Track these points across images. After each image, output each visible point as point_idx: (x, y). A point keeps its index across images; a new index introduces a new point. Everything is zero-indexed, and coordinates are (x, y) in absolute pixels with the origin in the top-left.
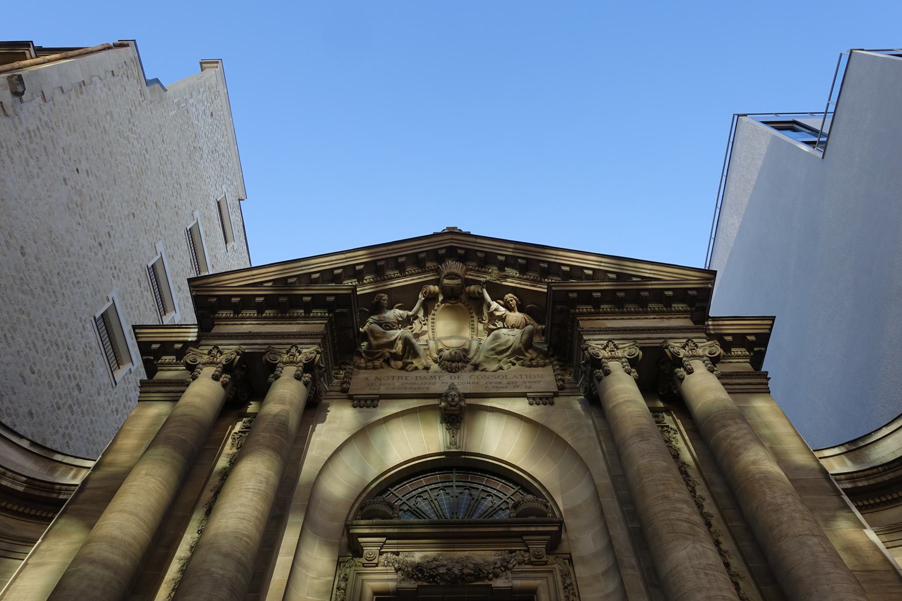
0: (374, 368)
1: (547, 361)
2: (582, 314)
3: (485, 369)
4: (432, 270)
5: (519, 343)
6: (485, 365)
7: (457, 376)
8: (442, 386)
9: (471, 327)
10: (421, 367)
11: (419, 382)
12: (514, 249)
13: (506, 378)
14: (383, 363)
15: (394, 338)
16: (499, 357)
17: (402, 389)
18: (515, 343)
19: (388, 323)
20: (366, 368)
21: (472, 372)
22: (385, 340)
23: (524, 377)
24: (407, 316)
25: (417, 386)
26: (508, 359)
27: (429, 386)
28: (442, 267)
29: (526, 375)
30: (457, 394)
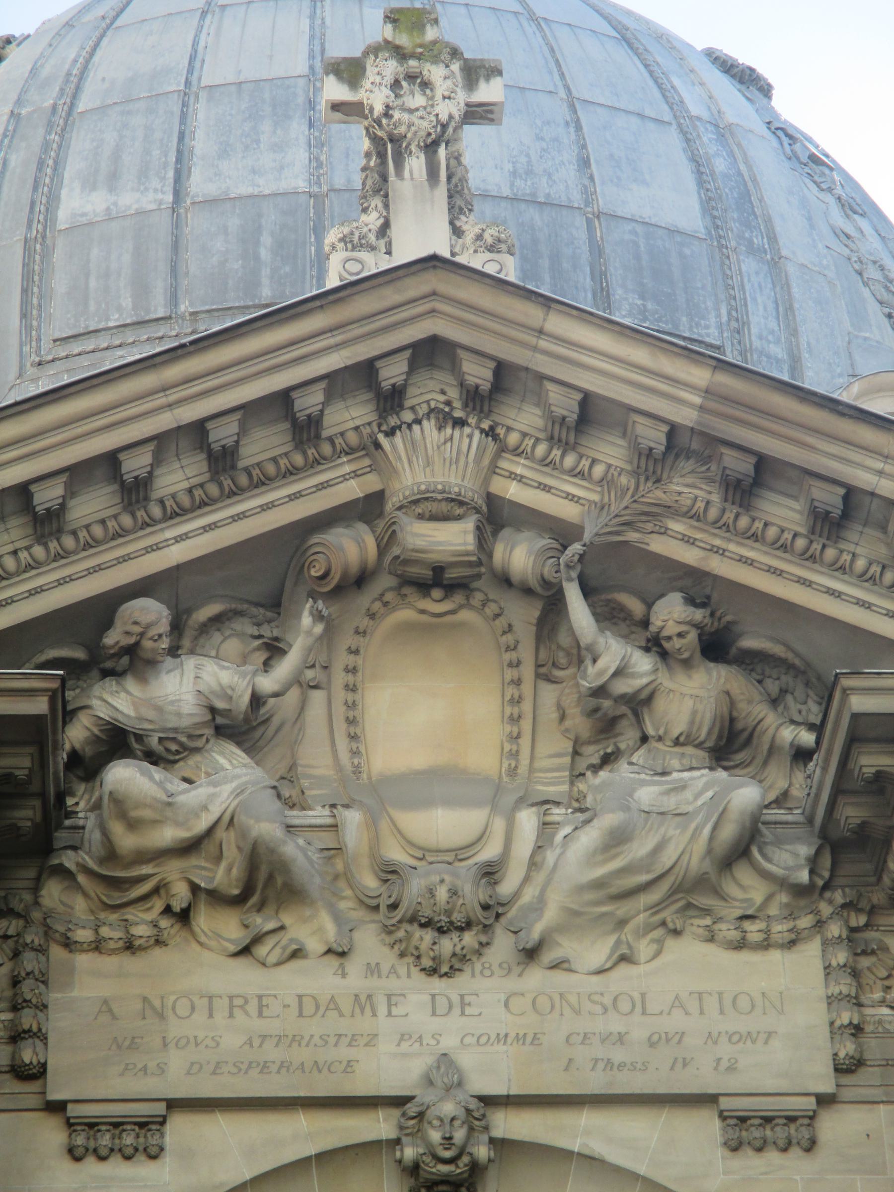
0: (130, 947)
1: (805, 922)
3: (565, 961)
4: (350, 451)
5: (703, 859)
7: (456, 999)
8: (404, 1055)
10: (314, 945)
11: (313, 1028)
13: (644, 1013)
14: (164, 923)
15: (202, 824)
16: (622, 909)
17: (254, 1073)
18: (686, 858)
19: (175, 730)
20: (97, 946)
21: (517, 970)
23: (712, 1004)
24: (257, 700)
28: (394, 447)
29: (720, 994)
30: (461, 1113)
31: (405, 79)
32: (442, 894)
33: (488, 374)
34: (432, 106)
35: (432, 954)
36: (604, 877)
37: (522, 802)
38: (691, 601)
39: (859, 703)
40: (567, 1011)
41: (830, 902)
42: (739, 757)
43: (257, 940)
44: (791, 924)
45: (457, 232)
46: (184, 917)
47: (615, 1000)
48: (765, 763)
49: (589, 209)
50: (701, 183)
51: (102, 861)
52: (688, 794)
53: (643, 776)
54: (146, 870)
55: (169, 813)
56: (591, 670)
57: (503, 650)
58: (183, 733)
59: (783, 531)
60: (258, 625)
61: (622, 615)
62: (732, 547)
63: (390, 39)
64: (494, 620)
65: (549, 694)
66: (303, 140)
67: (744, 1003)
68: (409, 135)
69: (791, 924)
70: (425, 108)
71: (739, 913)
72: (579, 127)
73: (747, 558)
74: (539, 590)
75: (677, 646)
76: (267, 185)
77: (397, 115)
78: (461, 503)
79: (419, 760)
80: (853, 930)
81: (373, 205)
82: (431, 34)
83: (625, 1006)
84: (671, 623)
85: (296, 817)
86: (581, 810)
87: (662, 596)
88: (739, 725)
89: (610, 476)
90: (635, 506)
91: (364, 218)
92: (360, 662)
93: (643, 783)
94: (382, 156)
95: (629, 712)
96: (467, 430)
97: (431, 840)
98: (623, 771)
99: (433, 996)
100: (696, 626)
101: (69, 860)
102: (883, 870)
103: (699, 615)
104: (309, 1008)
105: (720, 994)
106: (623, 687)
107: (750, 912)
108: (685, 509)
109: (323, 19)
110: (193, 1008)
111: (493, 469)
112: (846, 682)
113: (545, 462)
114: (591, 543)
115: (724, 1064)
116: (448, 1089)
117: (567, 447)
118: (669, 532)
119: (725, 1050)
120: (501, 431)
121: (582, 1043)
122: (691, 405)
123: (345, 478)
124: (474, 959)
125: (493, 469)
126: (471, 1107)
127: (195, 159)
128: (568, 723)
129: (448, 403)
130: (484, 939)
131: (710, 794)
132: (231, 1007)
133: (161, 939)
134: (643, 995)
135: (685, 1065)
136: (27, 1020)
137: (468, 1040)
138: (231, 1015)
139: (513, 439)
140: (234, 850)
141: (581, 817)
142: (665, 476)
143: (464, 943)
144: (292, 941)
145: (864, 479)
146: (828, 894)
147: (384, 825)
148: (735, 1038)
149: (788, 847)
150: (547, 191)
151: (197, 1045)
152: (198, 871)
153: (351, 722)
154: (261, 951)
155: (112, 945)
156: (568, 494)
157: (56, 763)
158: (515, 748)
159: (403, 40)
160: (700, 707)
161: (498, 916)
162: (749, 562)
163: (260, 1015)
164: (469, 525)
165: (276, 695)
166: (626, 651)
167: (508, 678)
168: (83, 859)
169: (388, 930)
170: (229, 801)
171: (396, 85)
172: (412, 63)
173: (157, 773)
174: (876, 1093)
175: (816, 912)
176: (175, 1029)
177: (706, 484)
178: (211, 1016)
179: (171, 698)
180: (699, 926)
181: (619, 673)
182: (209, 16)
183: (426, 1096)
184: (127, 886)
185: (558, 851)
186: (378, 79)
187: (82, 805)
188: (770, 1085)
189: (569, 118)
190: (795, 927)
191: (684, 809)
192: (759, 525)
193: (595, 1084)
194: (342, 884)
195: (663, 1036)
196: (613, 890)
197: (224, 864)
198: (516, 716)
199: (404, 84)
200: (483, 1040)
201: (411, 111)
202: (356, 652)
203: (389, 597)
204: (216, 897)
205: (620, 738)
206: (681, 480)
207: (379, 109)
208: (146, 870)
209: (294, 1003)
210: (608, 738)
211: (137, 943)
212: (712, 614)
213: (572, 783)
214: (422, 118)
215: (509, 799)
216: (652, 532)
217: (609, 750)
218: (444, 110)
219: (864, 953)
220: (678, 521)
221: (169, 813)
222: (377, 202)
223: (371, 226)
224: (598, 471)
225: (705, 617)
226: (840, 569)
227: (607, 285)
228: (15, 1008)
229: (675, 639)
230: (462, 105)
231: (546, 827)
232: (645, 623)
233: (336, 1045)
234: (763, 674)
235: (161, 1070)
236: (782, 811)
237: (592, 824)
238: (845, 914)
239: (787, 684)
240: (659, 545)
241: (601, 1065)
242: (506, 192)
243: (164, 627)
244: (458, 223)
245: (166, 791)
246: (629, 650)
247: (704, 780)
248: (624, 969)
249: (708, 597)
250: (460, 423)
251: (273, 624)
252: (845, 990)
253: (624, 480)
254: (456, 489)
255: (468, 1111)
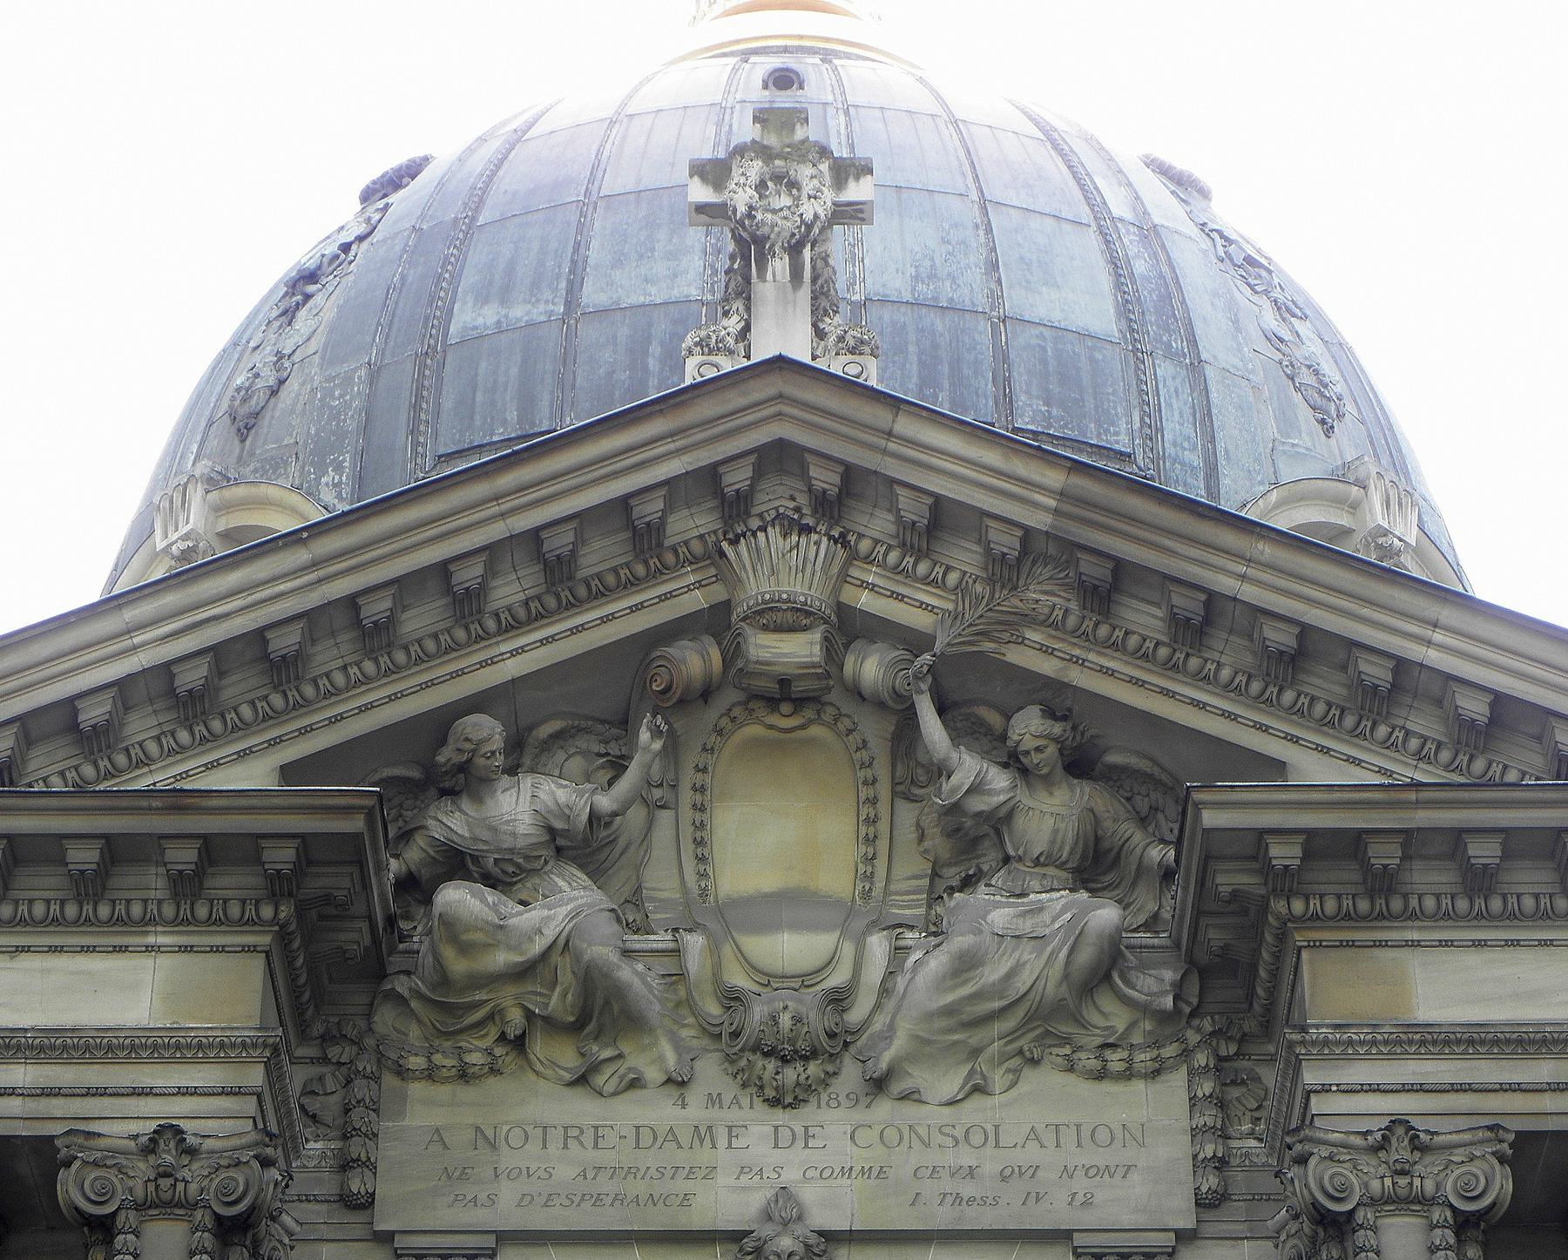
0: (464, 1075)
1: (1170, 1051)
2: (1315, 919)
4: (694, 560)
6: (915, 1071)
7: (799, 1130)
9: (863, 830)
12: (1063, 495)
13: (997, 1145)
14: (498, 1051)
15: (538, 946)
16: (975, 1038)
17: (587, 1205)
19: (511, 851)
21: (865, 1100)
22: (501, 959)
23: (1069, 1137)
24: (594, 818)
25: (638, 1187)
26: (1010, 1042)
27: (688, 1186)
28: (738, 554)
29: (1078, 1126)
30: (800, 1249)
31: (771, 179)
32: (785, 1021)
33: (836, 479)
34: (797, 206)
35: (775, 1084)
36: (952, 1003)
37: (874, 926)
38: (1050, 714)
39: (1210, 818)
40: (916, 1143)
41: (1199, 1030)
42: (1107, 878)
43: (595, 1067)
44: (1155, 1052)
45: (820, 334)
46: (519, 1044)
47: (967, 1132)
48: (1134, 884)
49: (995, 314)
50: (1119, 286)
51: (434, 987)
52: (1046, 917)
53: (998, 898)
54: (480, 996)
55: (500, 936)
56: (946, 787)
57: (858, 767)
58: (518, 854)
59: (1145, 640)
60: (606, 743)
61: (983, 730)
62: (1092, 657)
63: (758, 139)
64: (847, 735)
65: (907, 814)
66: (698, 247)
67: (1102, 1135)
68: (772, 236)
69: (1155, 1052)
70: (789, 208)
71: (1099, 1041)
72: (989, 230)
73: (1108, 668)
74: (890, 703)
75: (1036, 761)
76: (657, 294)
77: (759, 217)
78: (808, 614)
79: (769, 882)
80: (1220, 1059)
81: (734, 308)
82: (800, 133)
83: (977, 1139)
84: (1027, 736)
85: (636, 941)
86: (935, 934)
87: (1022, 708)
88: (1106, 845)
89: (964, 583)
90: (990, 614)
91: (725, 322)
92: (708, 780)
93: (997, 905)
94: (746, 259)
95: (992, 832)
96: (814, 537)
97: (776, 966)
98: (982, 893)
99: (776, 1128)
100: (1056, 740)
101: (401, 985)
102: (1252, 997)
103: (1058, 729)
104: (646, 1139)
105: (1078, 1126)
106: (978, 804)
107: (1111, 1040)
108: (1042, 617)
109: (731, 126)
110: (527, 1138)
111: (844, 577)
112: (1197, 796)
113: (897, 570)
114: (942, 653)
115: (1080, 1198)
116: (785, 1223)
117: (920, 555)
118: (1026, 642)
119: (1080, 1185)
120: (852, 538)
121: (931, 1177)
122: (1046, 509)
123: (689, 588)
124: (820, 1090)
125: (844, 577)
126: (810, 1242)
127: (588, 270)
128: (927, 844)
129: (797, 510)
130: (830, 1069)
131: (1068, 916)
132: (566, 1138)
133: (496, 1067)
134: (997, 1127)
135: (1038, 1200)
136: (356, 1148)
137: (810, 1174)
138: (566, 1146)
139: (865, 546)
140: (570, 975)
141: (933, 940)
142: (1021, 583)
143: (809, 1072)
144: (630, 1070)
145: (1225, 584)
146: (1196, 1022)
147: (728, 951)
148: (1092, 1172)
149: (1152, 972)
150: (950, 295)
151: (529, 1176)
152: (534, 997)
153: (699, 843)
154: (599, 1080)
155: (445, 1073)
156: (922, 603)
157: (381, 884)
158: (869, 869)
159: (772, 140)
160: (1062, 826)
161: (846, 1045)
162: (1111, 673)
163: (596, 1146)
164: (816, 636)
165: (615, 814)
166: (982, 767)
167: (863, 796)
168: (416, 984)
169: (730, 1059)
170: (563, 924)
171: (761, 186)
172: (778, 162)
173: (491, 896)
174: (1240, 1229)
175: (1183, 1041)
176: (508, 1159)
177: (1065, 591)
178: (545, 1147)
179: (506, 818)
180: (1058, 1055)
181: (974, 789)
182: (617, 126)
183: (767, 1230)
184: (460, 1013)
185: (908, 976)
186: (742, 180)
187: (420, 929)
188: (1127, 1220)
189: (979, 221)
190: (1159, 1055)
191: (1040, 932)
192: (1119, 633)
193: (942, 1217)
194: (684, 1011)
195: (1017, 1169)
196: (965, 1017)
197: (558, 989)
198: (871, 836)
199: (769, 184)
200: (826, 1174)
201: (774, 212)
202: (704, 770)
203: (736, 712)
204: (551, 1025)
205: (983, 859)
206: (1039, 587)
207: (742, 209)
208: (480, 996)
209: (632, 1135)
210: (970, 860)
211: (471, 1071)
212: (1074, 728)
213: (930, 907)
214: (785, 218)
215: (859, 924)
216: (1009, 642)
217: (971, 872)
218: (808, 209)
219: (1233, 1082)
220: (1035, 630)
221: (500, 936)
222: (738, 305)
223: (731, 330)
224: (953, 578)
225: (1065, 731)
226: (1203, 679)
227: (1011, 391)
228: (345, 1137)
229: (1032, 753)
230: (829, 204)
231: (899, 952)
232: (1004, 737)
233: (672, 1178)
234: (1132, 790)
235: (492, 1200)
236: (1148, 935)
237: (941, 948)
238: (1214, 1043)
239: (1157, 801)
240: (1016, 656)
241: (949, 1200)
242: (907, 297)
243: (497, 743)
244: (821, 326)
245: (497, 912)
246: (985, 765)
247: (1063, 901)
248: (977, 1101)
249: (1070, 710)
250: (806, 530)
251: (621, 742)
252: (1210, 1122)
253: (979, 588)
254: (802, 599)
255: (807, 1246)
